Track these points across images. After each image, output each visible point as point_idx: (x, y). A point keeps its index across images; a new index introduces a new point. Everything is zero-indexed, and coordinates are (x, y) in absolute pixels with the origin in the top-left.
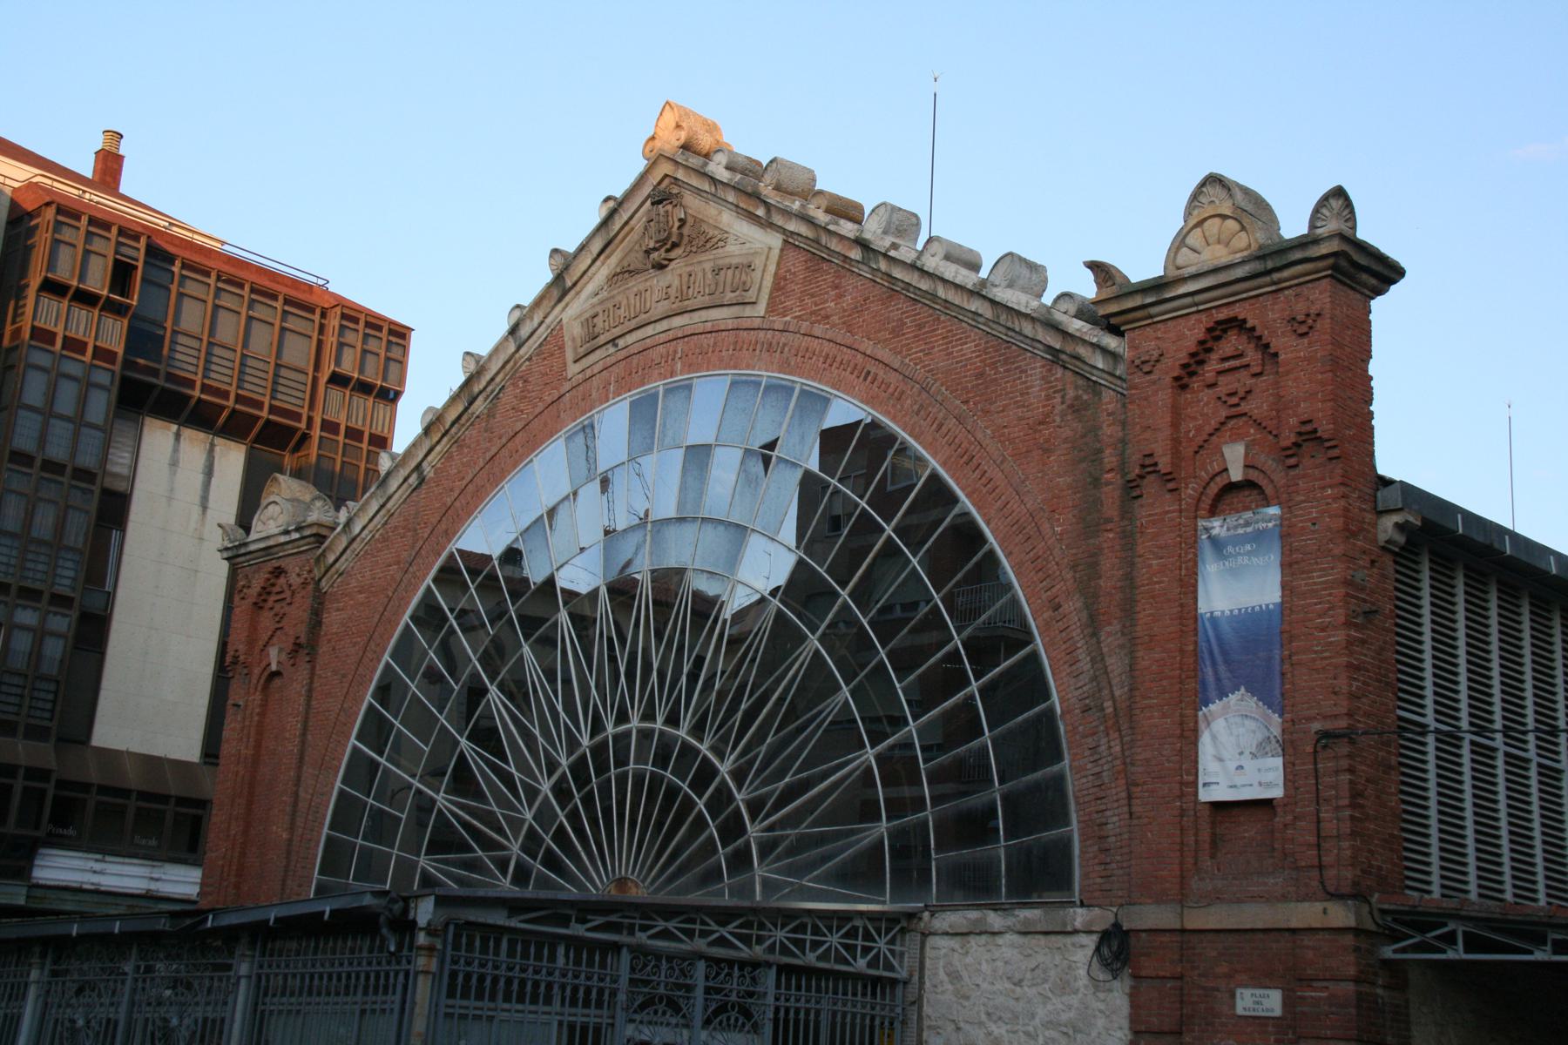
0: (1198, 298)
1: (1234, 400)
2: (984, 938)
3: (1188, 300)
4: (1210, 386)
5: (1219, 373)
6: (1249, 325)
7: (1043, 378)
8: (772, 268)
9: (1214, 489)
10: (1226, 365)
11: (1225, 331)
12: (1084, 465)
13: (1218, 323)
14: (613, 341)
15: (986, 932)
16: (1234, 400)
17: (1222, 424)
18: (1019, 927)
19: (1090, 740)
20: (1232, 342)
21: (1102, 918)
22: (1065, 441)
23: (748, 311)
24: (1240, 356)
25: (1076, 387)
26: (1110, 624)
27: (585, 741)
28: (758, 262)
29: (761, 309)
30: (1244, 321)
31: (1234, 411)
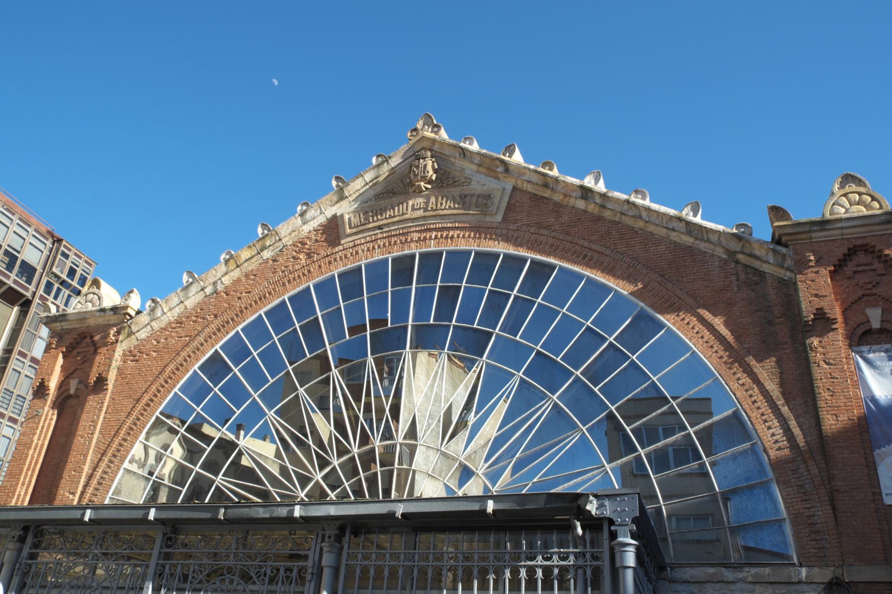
0: (845, 231)
1: (870, 286)
2: (718, 586)
3: (839, 232)
4: (849, 278)
5: (854, 272)
6: (877, 249)
7: (721, 267)
8: (506, 199)
9: (860, 331)
10: (860, 268)
11: (855, 252)
12: (760, 313)
13: (855, 246)
14: (380, 228)
15: (723, 581)
16: (870, 286)
17: (859, 298)
18: (750, 579)
19: (791, 465)
20: (861, 258)
21: (824, 575)
22: (743, 299)
23: (488, 219)
24: (870, 264)
25: (746, 273)
26: (794, 400)
27: (356, 450)
28: (498, 195)
29: (499, 218)
30: (874, 246)
31: (868, 292)
